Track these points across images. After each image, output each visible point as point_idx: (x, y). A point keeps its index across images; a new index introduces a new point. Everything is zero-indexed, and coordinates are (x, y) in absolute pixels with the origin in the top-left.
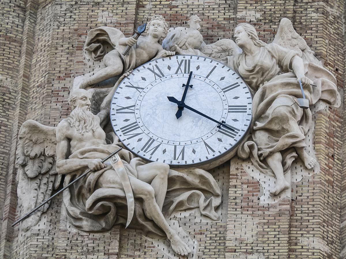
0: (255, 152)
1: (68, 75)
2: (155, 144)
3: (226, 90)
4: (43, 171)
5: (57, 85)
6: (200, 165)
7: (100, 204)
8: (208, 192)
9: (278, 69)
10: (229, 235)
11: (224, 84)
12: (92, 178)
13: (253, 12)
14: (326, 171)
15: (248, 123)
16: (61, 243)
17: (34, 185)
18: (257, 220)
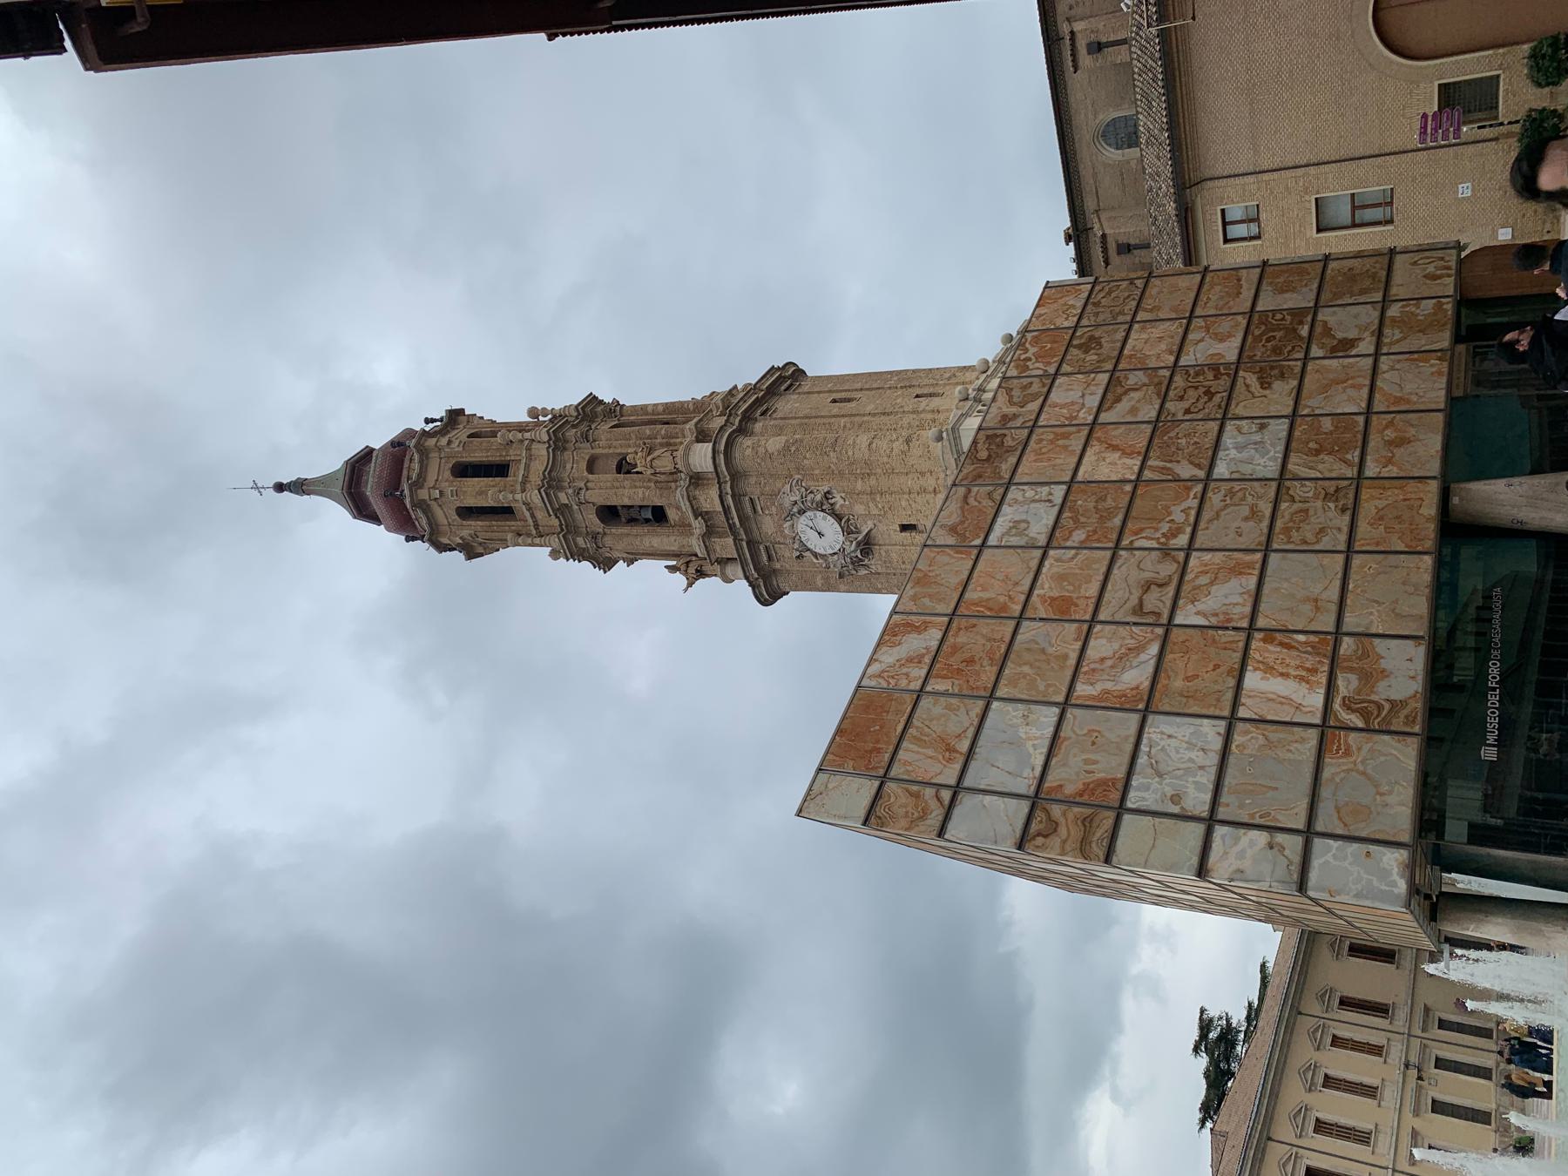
6: (840, 525)
8: (848, 520)
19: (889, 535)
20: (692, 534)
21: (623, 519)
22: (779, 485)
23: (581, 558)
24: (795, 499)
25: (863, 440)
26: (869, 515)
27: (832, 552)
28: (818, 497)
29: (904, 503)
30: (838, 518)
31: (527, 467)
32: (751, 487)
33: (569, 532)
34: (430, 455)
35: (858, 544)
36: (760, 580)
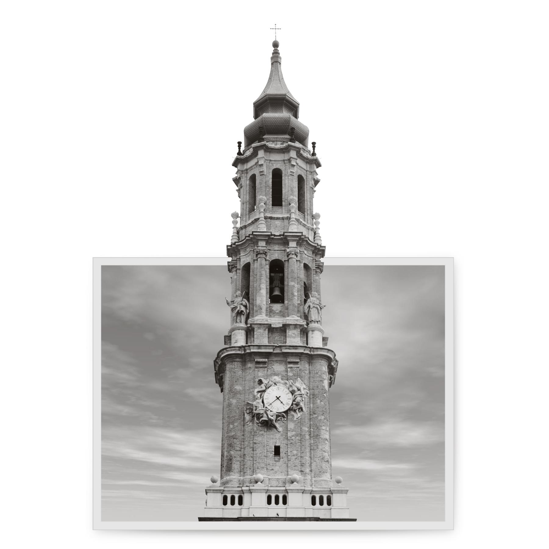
0: (293, 408)
1: (253, 388)
2: (273, 407)
3: (287, 394)
4: (250, 411)
5: (251, 390)
7: (263, 421)
8: (284, 417)
9: (297, 390)
10: (289, 427)
11: (286, 393)
12: (261, 415)
13: (291, 374)
14: (307, 412)
15: (292, 402)
16: (255, 429)
17: (249, 415)
18: (294, 424)
19: (273, 439)
20: (266, 315)
21: (273, 274)
22: (306, 382)
23: (247, 238)
24: (302, 389)
25: (327, 437)
26: (286, 430)
27: (265, 401)
28: (302, 404)
29: (295, 452)
30: (286, 412)
31: (304, 225)
32: (304, 365)
33: (269, 238)
34: (308, 164)
35: (271, 420)
36: (243, 352)
